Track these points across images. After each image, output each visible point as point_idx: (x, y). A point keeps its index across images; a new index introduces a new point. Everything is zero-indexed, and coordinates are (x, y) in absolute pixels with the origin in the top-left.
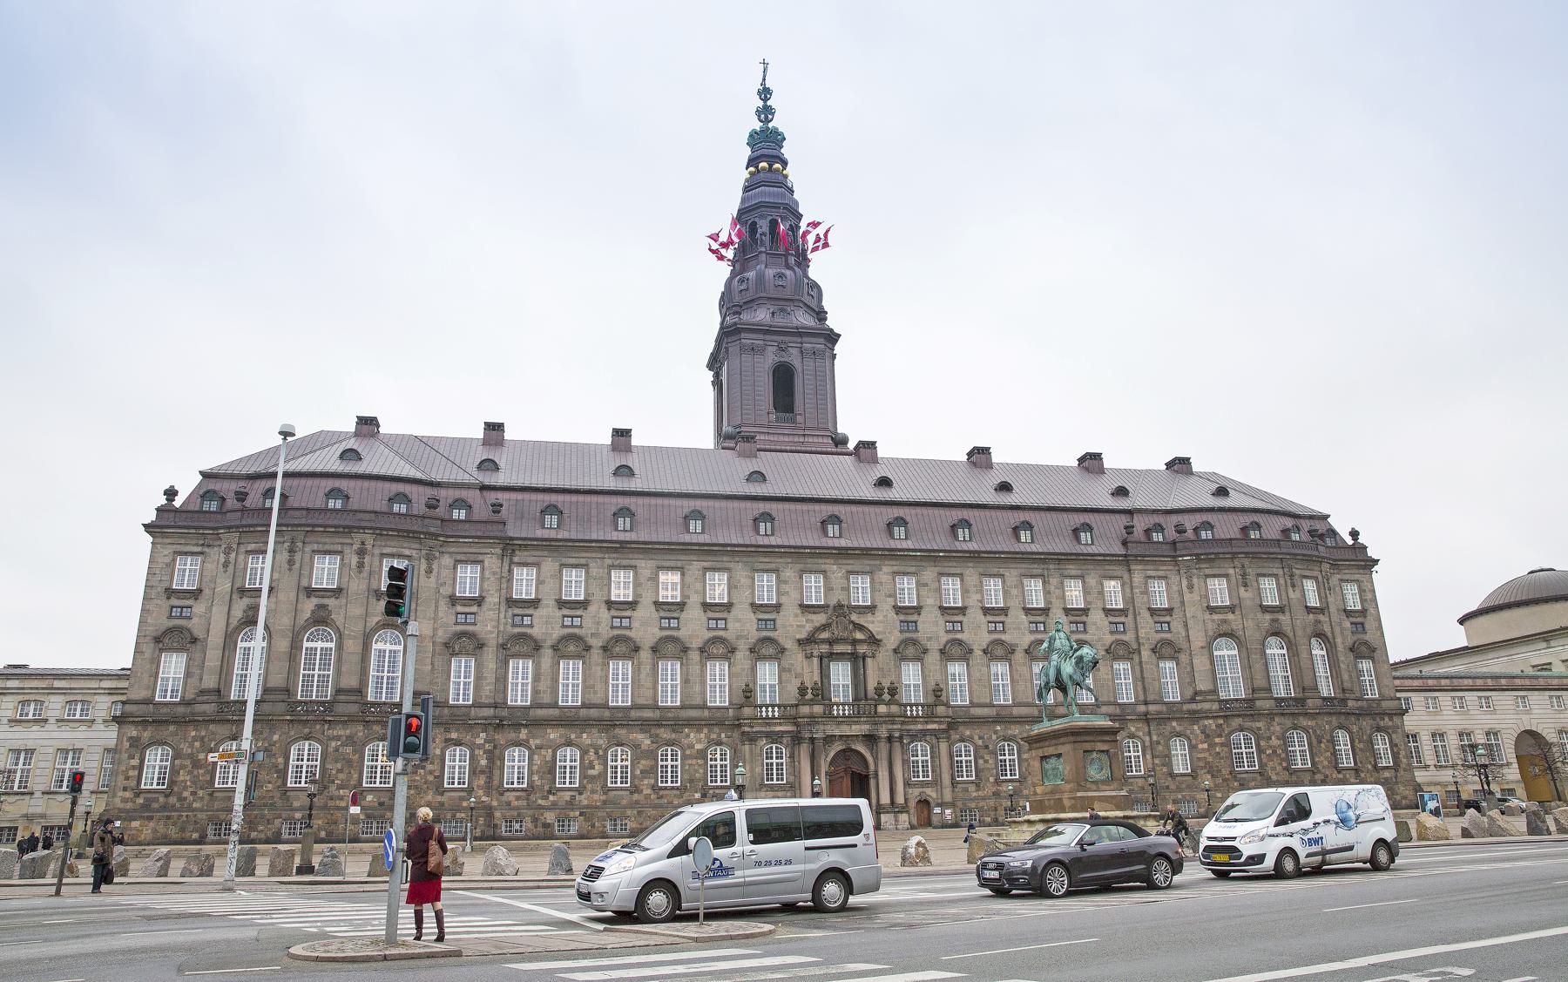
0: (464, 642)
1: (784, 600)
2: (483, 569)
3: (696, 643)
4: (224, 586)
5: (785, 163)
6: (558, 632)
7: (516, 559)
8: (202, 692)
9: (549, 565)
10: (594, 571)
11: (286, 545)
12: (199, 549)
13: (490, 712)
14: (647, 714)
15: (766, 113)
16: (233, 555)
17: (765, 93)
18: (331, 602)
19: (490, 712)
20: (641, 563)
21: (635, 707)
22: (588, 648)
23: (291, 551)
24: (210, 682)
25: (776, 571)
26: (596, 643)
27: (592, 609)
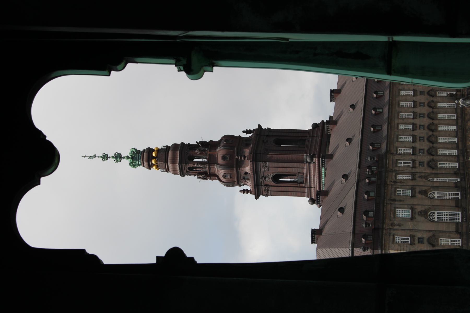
0: (432, 165)
1: (412, 89)
2: (399, 160)
3: (430, 110)
4: (410, 225)
5: (150, 151)
6: (426, 142)
7: (395, 153)
8: (457, 232)
9: (397, 144)
10: (399, 133)
11: (392, 202)
12: (392, 237)
13: (461, 158)
14: (460, 121)
15: (118, 157)
16: (396, 222)
17: (105, 157)
18: (418, 190)
19: (461, 158)
20: (396, 121)
21: (457, 124)
22: (433, 135)
23: (395, 200)
24: (453, 228)
25: (399, 90)
26: (430, 133)
27: (416, 134)
